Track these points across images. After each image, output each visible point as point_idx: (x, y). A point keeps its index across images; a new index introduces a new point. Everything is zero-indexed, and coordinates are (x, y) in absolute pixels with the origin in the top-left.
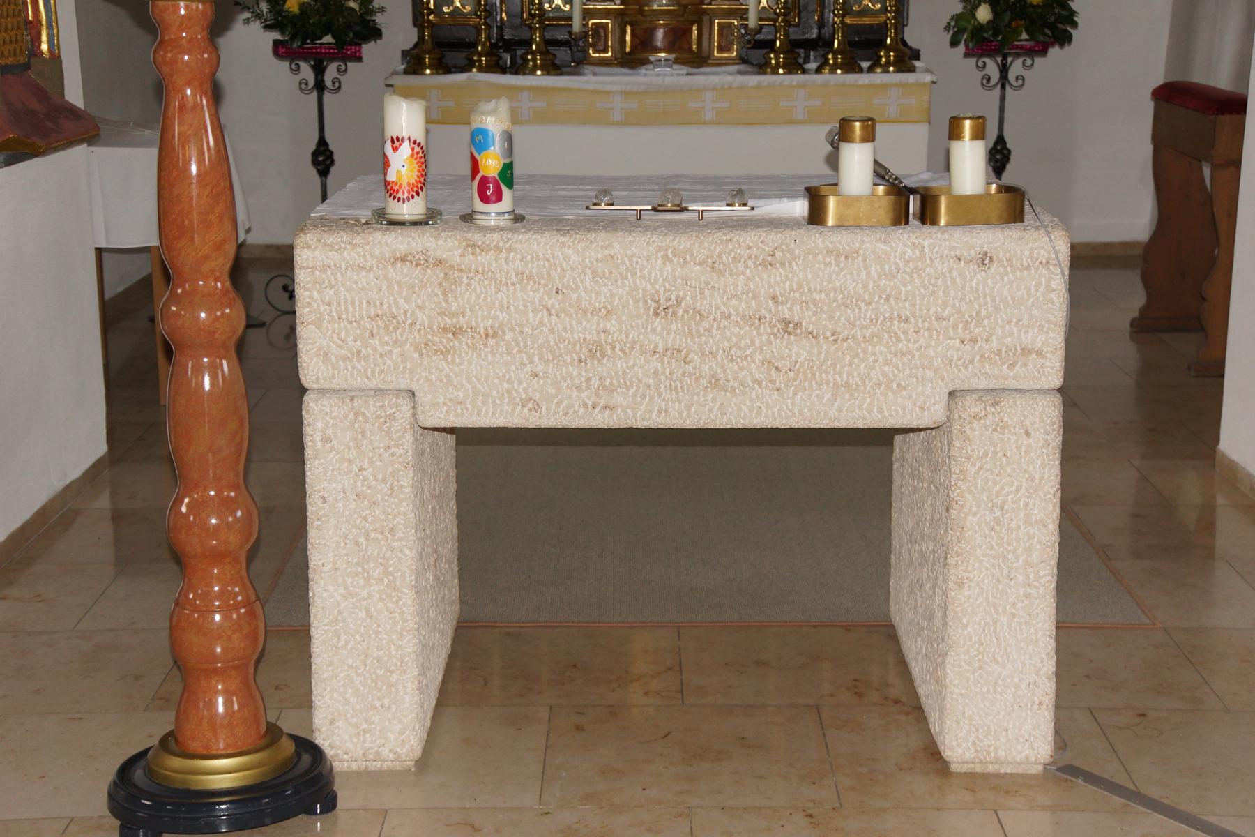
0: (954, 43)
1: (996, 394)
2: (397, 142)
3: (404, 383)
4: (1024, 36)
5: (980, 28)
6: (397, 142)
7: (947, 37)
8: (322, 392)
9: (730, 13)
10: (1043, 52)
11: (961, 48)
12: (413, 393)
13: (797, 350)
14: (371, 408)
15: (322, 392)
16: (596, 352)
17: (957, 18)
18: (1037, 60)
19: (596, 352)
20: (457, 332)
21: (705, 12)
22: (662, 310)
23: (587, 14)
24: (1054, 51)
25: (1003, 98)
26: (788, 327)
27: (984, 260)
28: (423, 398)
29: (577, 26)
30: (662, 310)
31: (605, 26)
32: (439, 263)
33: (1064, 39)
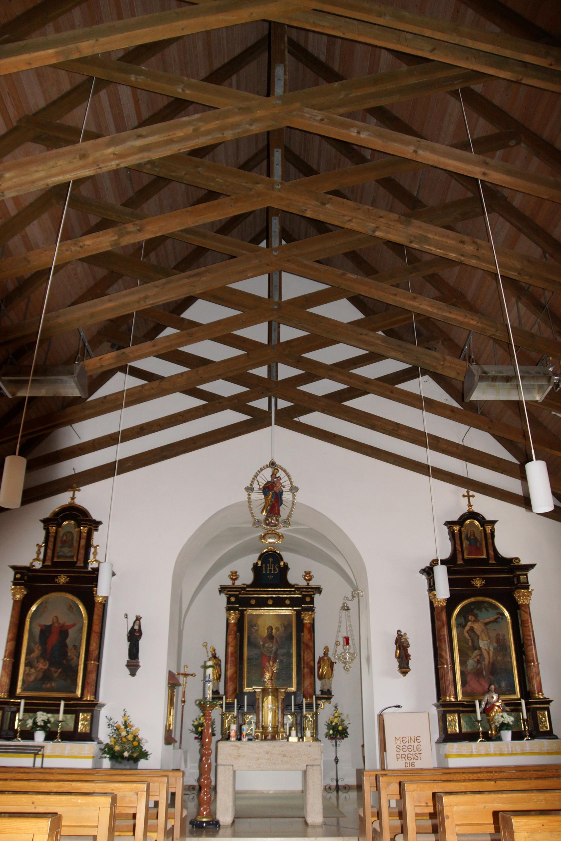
0: (326, 737)
1: (313, 765)
2: (232, 730)
3: (232, 764)
4: (339, 736)
5: (330, 735)
6: (232, 730)
7: (324, 736)
8: (221, 765)
9: (283, 732)
10: (343, 739)
11: (327, 738)
12: (232, 765)
13: (285, 759)
14: (227, 767)
15: (221, 765)
16: (258, 759)
17: (327, 733)
18: (342, 740)
19: (258, 759)
20: (239, 756)
21: (278, 732)
22: (267, 753)
23: (256, 732)
24: (345, 739)
25: (336, 749)
26: (284, 755)
27: (310, 746)
28: (234, 766)
29: (253, 735)
30: (267, 753)
31: (258, 735)
32: (237, 746)
33: (346, 737)
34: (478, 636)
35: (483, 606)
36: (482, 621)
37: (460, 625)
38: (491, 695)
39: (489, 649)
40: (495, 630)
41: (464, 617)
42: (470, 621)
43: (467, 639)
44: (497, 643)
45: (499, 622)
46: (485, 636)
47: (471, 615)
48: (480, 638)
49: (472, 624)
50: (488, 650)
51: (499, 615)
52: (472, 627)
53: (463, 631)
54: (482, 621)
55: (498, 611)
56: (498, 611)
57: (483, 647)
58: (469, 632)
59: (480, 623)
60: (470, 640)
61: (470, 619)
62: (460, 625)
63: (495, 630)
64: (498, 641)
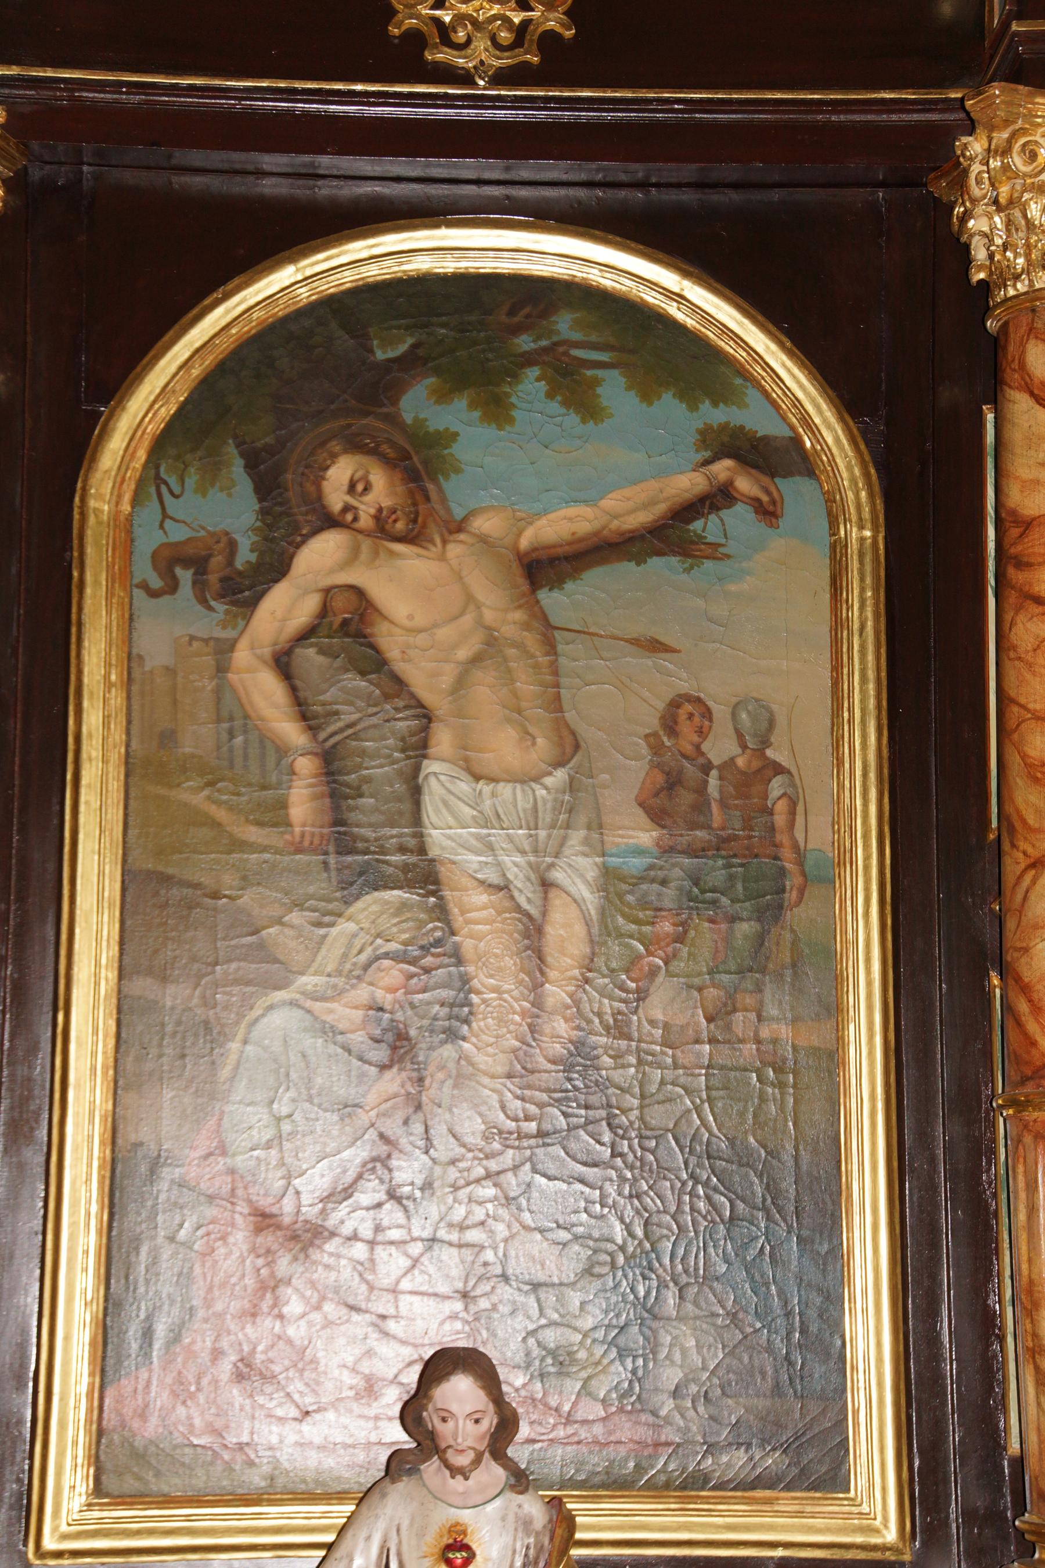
34: (426, 717)
35: (525, 343)
36: (486, 524)
37: (199, 564)
38: (445, 1515)
39: (546, 885)
40: (655, 646)
41: (252, 464)
42: (330, 522)
43: (282, 751)
44: (657, 816)
45: (714, 552)
46: (515, 711)
47: (355, 446)
48: (443, 739)
49: (353, 556)
50: (526, 896)
51: (723, 468)
52: (358, 592)
53: (224, 650)
54: (486, 524)
55: (717, 415)
56: (717, 415)
57: (472, 860)
58: (309, 656)
59: (454, 550)
60: (306, 765)
61: (336, 499)
62: (199, 564)
63: (655, 646)
64: (673, 782)
